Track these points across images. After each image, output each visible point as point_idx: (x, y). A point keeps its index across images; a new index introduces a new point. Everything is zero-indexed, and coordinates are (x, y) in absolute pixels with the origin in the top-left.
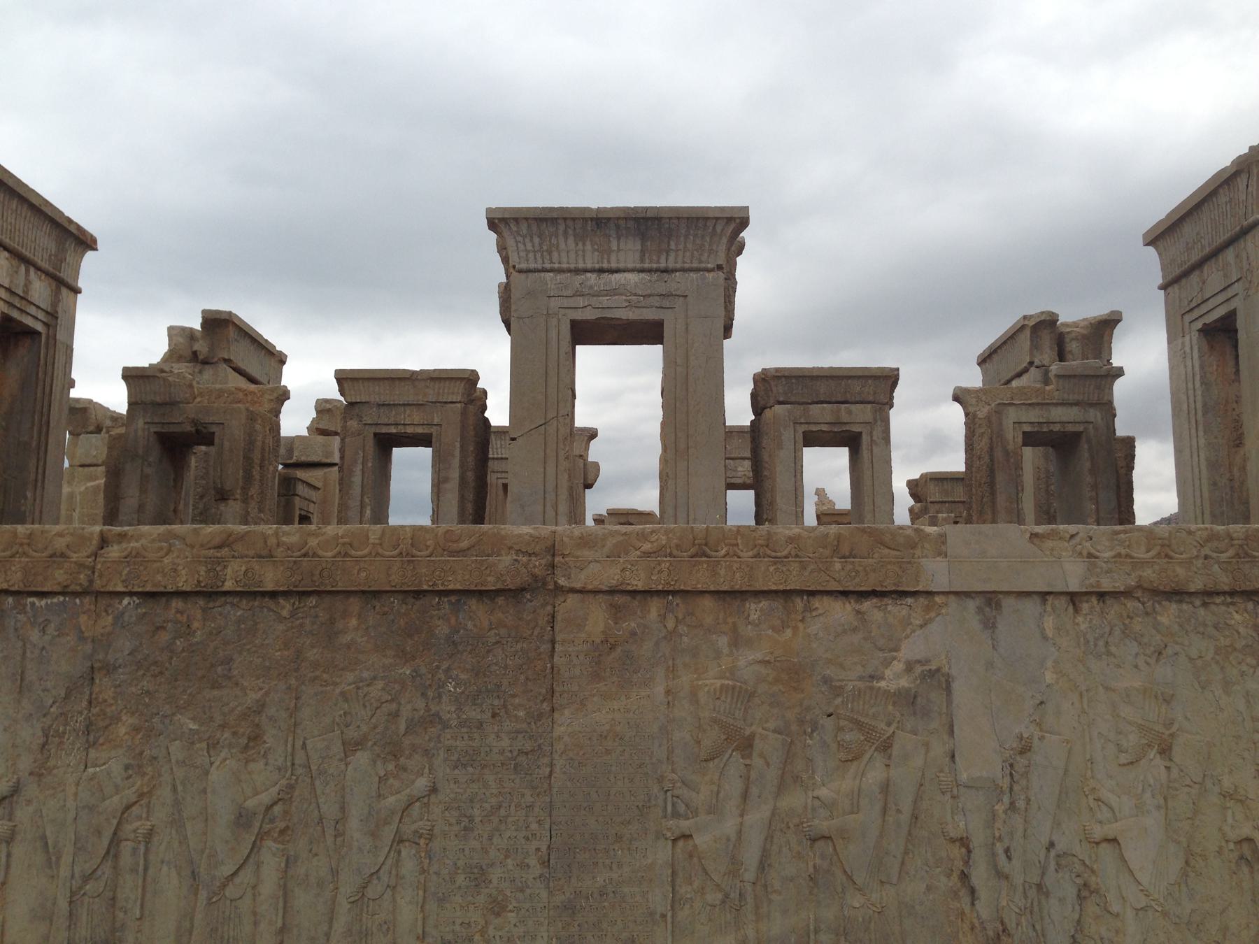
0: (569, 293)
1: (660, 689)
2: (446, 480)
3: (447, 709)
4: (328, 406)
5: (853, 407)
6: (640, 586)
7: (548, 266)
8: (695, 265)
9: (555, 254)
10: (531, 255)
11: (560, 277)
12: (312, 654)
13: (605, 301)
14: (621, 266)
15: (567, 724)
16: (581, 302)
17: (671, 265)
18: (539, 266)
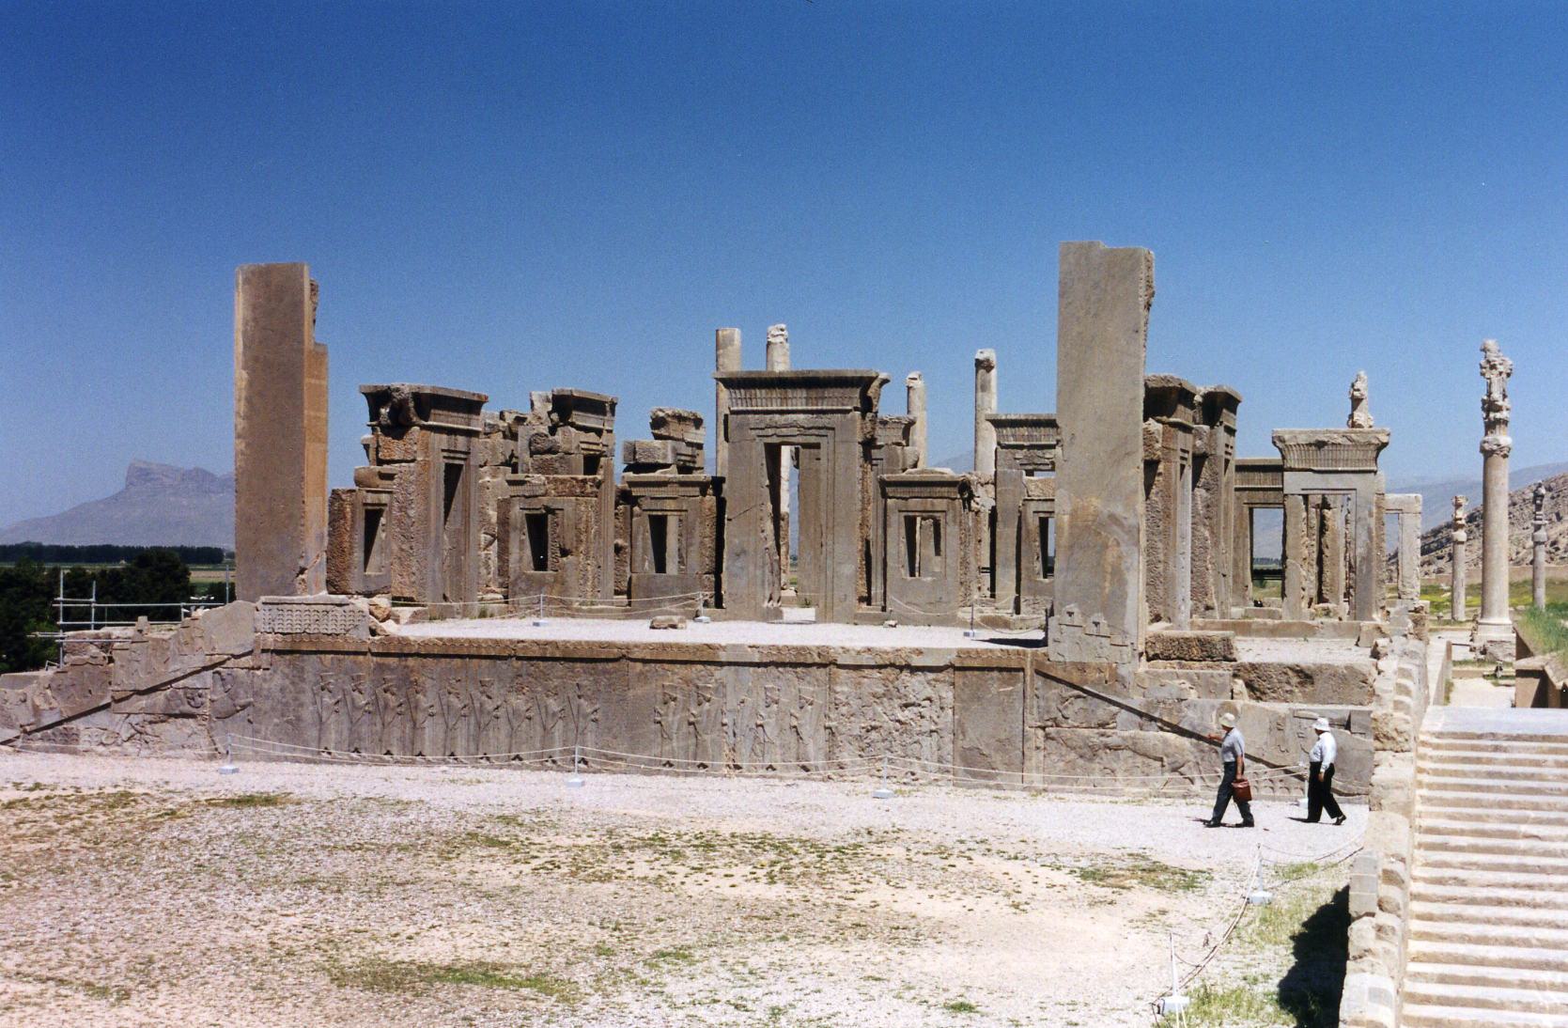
0: (763, 426)
1: (654, 686)
2: (691, 545)
3: (602, 688)
4: (661, 414)
5: (935, 501)
6: (648, 657)
7: (749, 408)
8: (840, 408)
9: (754, 402)
10: (739, 402)
11: (757, 416)
12: (570, 674)
13: (785, 431)
14: (794, 408)
15: (631, 693)
16: (770, 432)
17: (825, 408)
18: (744, 408)
